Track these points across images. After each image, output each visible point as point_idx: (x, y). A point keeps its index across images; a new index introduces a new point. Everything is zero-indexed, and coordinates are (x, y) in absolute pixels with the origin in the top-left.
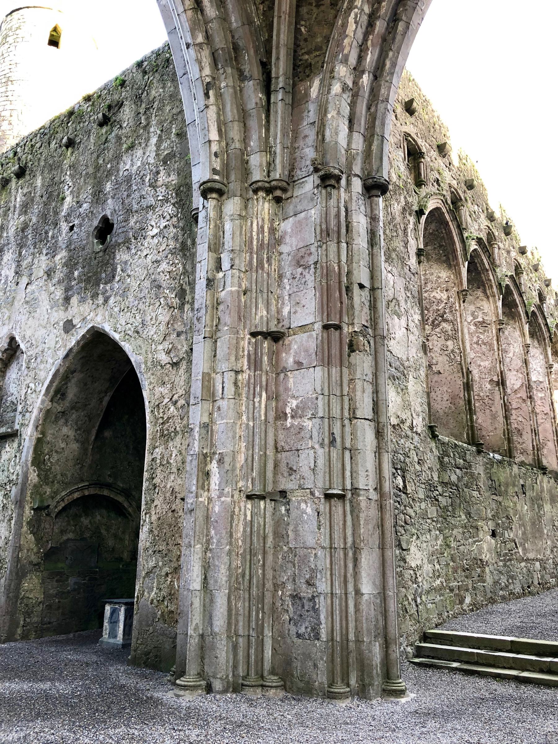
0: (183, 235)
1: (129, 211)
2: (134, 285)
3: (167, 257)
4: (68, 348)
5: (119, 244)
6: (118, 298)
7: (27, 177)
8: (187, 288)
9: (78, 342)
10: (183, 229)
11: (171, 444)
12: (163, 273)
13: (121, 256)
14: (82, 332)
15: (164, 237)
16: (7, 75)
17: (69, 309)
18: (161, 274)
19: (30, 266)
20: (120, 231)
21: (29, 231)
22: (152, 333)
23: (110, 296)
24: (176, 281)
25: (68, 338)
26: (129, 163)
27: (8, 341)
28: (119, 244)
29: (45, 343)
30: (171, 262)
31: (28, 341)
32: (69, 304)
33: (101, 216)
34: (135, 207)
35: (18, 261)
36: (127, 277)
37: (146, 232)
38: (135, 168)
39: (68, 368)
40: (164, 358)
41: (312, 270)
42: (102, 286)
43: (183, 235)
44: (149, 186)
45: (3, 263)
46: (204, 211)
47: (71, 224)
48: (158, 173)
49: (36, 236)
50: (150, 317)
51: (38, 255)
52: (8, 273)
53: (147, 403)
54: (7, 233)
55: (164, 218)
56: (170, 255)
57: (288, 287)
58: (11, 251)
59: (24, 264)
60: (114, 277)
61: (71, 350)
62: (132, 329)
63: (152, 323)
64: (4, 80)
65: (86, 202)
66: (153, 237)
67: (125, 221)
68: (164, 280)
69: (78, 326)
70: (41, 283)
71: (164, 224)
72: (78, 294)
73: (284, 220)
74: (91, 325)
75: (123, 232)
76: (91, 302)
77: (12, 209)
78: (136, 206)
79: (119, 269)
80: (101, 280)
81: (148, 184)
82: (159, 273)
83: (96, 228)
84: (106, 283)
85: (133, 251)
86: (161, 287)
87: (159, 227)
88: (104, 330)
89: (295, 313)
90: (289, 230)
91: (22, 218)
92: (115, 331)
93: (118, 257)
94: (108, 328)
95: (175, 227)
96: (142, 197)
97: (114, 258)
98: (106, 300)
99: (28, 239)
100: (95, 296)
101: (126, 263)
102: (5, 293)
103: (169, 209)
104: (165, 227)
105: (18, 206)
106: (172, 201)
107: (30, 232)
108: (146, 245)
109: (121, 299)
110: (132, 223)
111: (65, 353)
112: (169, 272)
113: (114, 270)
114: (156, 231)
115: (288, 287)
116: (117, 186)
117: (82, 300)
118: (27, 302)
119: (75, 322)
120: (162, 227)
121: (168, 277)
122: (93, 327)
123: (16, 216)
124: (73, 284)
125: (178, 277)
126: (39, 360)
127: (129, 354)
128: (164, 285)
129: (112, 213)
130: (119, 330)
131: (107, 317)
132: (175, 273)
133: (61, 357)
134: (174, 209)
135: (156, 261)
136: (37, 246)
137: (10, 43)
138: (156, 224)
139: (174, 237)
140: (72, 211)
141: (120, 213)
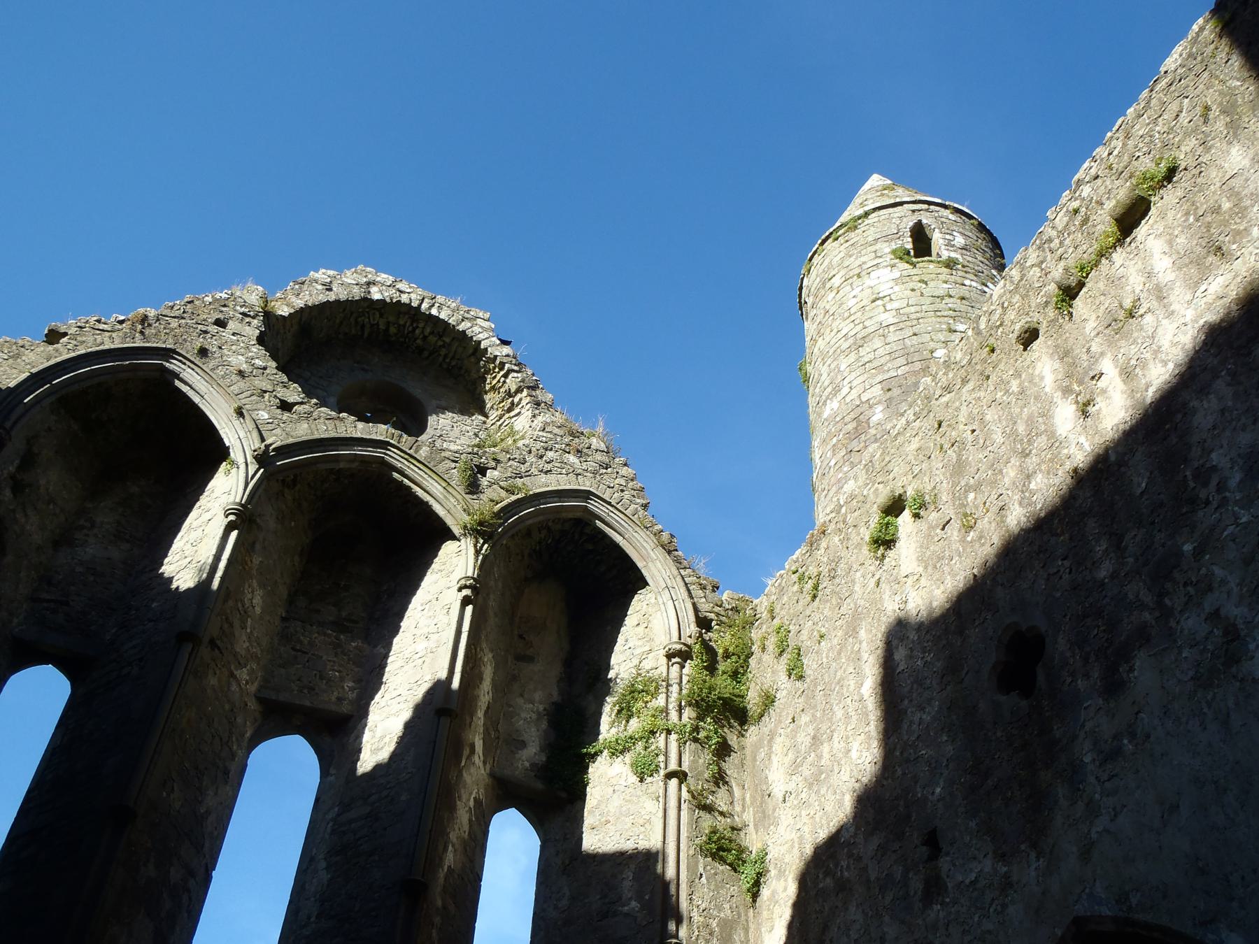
16: (852, 333)
58: (1220, 385)
64: (846, 345)
137: (837, 285)
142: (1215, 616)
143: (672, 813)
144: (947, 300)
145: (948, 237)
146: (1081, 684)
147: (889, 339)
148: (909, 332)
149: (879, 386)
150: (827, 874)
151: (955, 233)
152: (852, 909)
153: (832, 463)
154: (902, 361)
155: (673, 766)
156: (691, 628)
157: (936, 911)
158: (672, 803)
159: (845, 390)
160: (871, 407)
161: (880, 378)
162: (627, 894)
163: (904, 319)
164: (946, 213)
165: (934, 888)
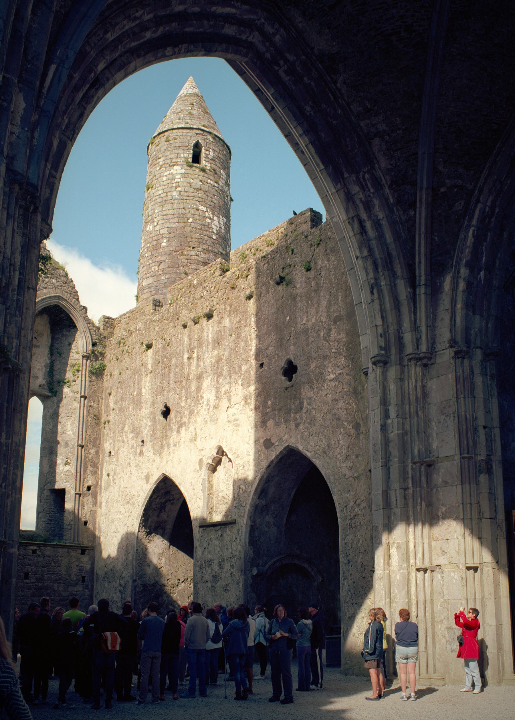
0: (355, 382)
1: (309, 358)
2: (319, 417)
3: (343, 397)
4: (269, 460)
5: (304, 383)
6: (307, 425)
7: (215, 318)
8: (361, 423)
9: (277, 456)
10: (354, 377)
11: (358, 533)
12: (341, 409)
13: (306, 393)
14: (280, 449)
15: (339, 382)
17: (267, 430)
18: (340, 410)
19: (227, 392)
20: (303, 373)
21: (224, 362)
22: (336, 454)
23: (300, 423)
24: (352, 416)
25: (269, 453)
26: (305, 318)
27: (216, 451)
28: (304, 383)
29: (249, 455)
30: (347, 402)
31: (235, 453)
32: (267, 426)
33: (286, 359)
34: (314, 355)
35: (216, 387)
36: (312, 410)
37: (325, 376)
38: (310, 323)
39: (270, 474)
40: (348, 473)
41: (452, 418)
42: (292, 415)
43: (355, 382)
44: (324, 340)
45: (203, 388)
46: (373, 373)
47: (261, 363)
48: (330, 330)
49: (230, 368)
50: (334, 442)
51: (234, 384)
52: (209, 396)
53: (337, 504)
54: (204, 363)
55: (338, 367)
56: (345, 396)
57: (435, 429)
58: (209, 378)
59: (223, 390)
60: (301, 409)
61: (272, 462)
62: (321, 450)
63: (336, 446)
65: (271, 346)
66: (331, 381)
67: (307, 365)
68: (343, 414)
69: (276, 444)
70: (239, 407)
71: (339, 372)
72: (273, 419)
73: (430, 379)
74: (287, 444)
75: (305, 374)
76: (285, 426)
77: (206, 343)
78: (314, 354)
79: (305, 403)
80: (290, 410)
81: (322, 338)
82: (338, 409)
83: (282, 368)
84: (296, 413)
85: (316, 390)
86: (340, 419)
87: (335, 373)
88: (298, 449)
89: (442, 447)
90: (434, 387)
91: (216, 352)
92: (307, 450)
93: (303, 394)
94: (300, 448)
95: (347, 375)
96: (319, 348)
97: (300, 394)
98: (297, 425)
99: (223, 369)
100: (287, 421)
101: (310, 398)
102: (208, 413)
103: (342, 361)
104: (340, 374)
105: (210, 341)
106: (344, 354)
107: (224, 364)
108: (325, 385)
109: (310, 426)
110: (312, 367)
111: (267, 464)
112: (346, 409)
113: (302, 403)
114: (332, 376)
115: (435, 429)
116: (297, 336)
117: (277, 424)
118: (229, 422)
119: (273, 441)
120: (337, 374)
121: (345, 413)
122: (288, 446)
123: (210, 350)
124: (268, 410)
125: (353, 413)
126: (246, 468)
127: (320, 468)
128: (343, 418)
129: (295, 358)
130: (310, 450)
131: (299, 440)
132: (351, 410)
133: (265, 467)
134: (346, 361)
135: (335, 400)
136: (233, 377)
138: (333, 371)
139: (348, 382)
140: (260, 352)
141: (302, 358)
142: (195, 429)
143: (82, 408)
144: (200, 192)
145: (207, 153)
146: (174, 427)
147: (175, 206)
148: (181, 206)
149: (167, 229)
150: (120, 436)
151: (211, 150)
152: (125, 448)
153: (146, 255)
154: (176, 220)
155: (83, 394)
156: (90, 347)
157: (140, 458)
158: (82, 405)
159: (155, 224)
160: (162, 238)
161: (168, 225)
162: (69, 429)
163: (182, 198)
164: (209, 137)
165: (141, 453)
